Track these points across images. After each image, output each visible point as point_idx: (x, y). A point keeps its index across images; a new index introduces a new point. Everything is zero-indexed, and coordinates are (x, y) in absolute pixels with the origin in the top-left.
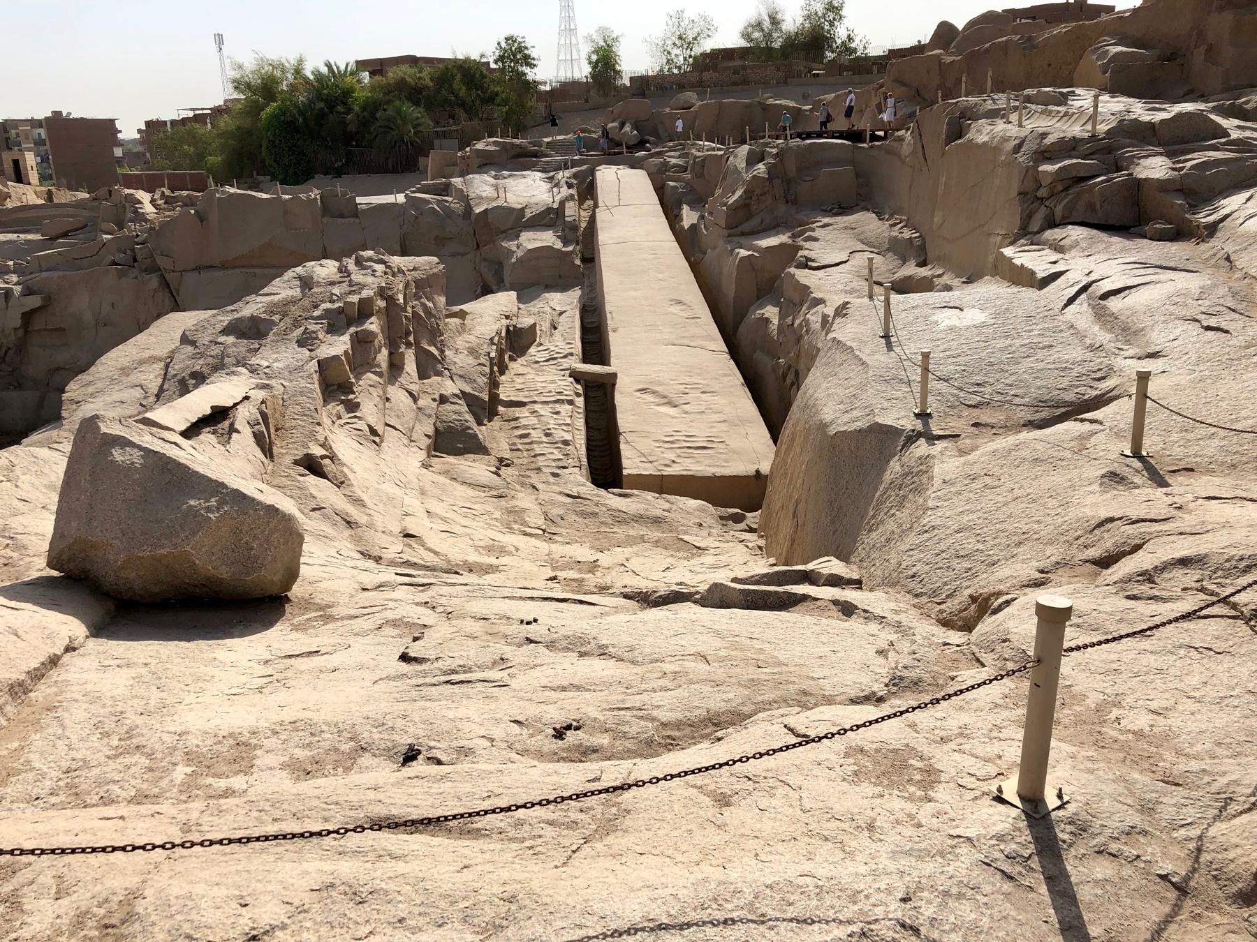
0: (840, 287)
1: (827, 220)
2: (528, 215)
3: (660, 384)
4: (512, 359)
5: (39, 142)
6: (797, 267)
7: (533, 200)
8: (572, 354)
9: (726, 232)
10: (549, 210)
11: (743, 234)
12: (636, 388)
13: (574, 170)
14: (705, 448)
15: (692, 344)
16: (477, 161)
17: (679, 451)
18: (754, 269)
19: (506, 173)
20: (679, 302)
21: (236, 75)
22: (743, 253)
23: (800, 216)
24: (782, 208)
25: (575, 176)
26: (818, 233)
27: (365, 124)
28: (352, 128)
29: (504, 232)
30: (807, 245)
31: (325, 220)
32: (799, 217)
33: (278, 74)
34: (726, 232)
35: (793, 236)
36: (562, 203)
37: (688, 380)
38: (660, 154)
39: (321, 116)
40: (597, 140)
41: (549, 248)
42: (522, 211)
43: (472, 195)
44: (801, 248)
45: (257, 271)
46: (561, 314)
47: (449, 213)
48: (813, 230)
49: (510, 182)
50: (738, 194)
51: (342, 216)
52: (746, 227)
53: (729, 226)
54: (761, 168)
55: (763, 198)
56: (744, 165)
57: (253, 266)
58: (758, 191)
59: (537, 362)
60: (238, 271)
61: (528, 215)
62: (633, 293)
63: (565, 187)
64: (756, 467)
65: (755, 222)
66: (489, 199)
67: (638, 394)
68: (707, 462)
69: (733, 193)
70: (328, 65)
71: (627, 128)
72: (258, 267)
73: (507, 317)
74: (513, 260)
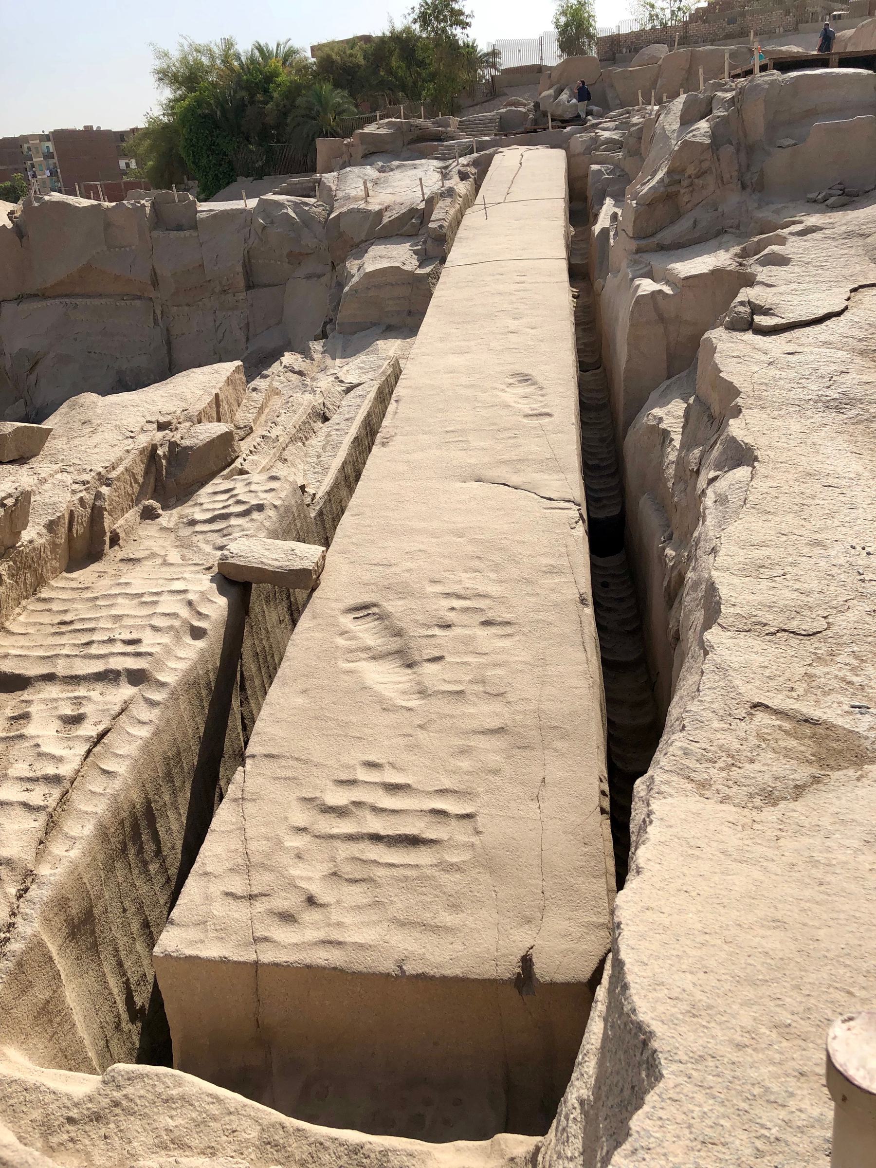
0: (815, 387)
1: (813, 220)
2: (386, 220)
3: (404, 591)
4: (149, 515)
5: (48, 156)
6: (733, 327)
7: (399, 200)
8: (260, 508)
9: (633, 245)
10: (412, 212)
11: (662, 248)
12: (352, 601)
13: (476, 155)
14: (413, 841)
15: (514, 480)
16: (360, 150)
17: (345, 850)
18: (661, 319)
19: (396, 163)
20: (525, 379)
21: (158, 64)
22: (647, 286)
23: (766, 214)
24: (733, 199)
25: (475, 163)
26: (793, 247)
27: (284, 114)
28: (270, 120)
29: (357, 245)
30: (763, 273)
31: (155, 234)
32: (761, 214)
33: (205, 60)
34: (633, 245)
35: (745, 254)
36: (431, 202)
37: (468, 581)
38: (596, 126)
39: (241, 108)
40: (525, 115)
41: (395, 270)
42: (380, 214)
43: (340, 194)
44: (750, 281)
45: (79, 301)
46: (348, 391)
47: (307, 220)
48: (782, 241)
49: (397, 174)
50: (660, 175)
51: (179, 228)
52: (667, 235)
53: (639, 235)
54: (703, 125)
55: (699, 182)
56: (676, 126)
57: (77, 296)
58: (691, 170)
59: (193, 523)
60: (57, 301)
61: (386, 220)
62: (455, 360)
63: (456, 178)
64: (521, 940)
65: (683, 225)
66: (356, 199)
67: (347, 621)
68: (400, 903)
69: (653, 175)
70: (259, 48)
71: (564, 96)
72: (82, 296)
73: (161, 427)
74: (347, 289)
